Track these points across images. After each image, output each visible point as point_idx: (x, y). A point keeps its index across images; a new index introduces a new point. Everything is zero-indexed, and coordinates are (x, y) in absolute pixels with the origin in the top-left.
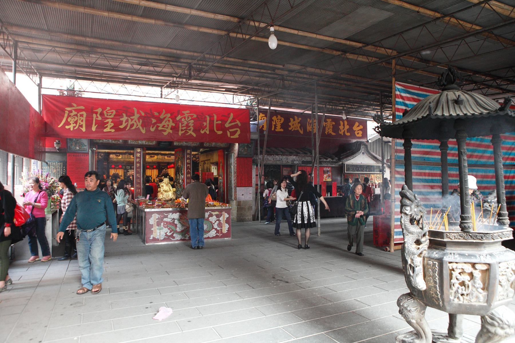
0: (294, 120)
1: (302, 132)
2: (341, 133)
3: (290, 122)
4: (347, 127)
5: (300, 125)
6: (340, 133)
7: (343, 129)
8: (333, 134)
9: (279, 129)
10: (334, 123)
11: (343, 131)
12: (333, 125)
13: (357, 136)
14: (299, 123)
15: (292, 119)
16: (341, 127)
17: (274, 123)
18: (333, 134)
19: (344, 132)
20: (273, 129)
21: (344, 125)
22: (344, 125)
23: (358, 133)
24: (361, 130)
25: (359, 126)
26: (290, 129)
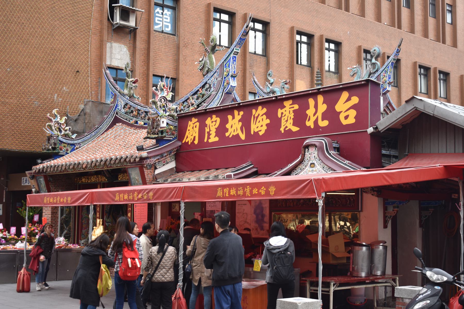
0: (233, 118)
1: (243, 137)
2: (310, 124)
3: (227, 122)
4: (322, 108)
5: (241, 123)
6: (308, 124)
7: (314, 115)
8: (295, 129)
9: (214, 139)
10: (296, 107)
11: (313, 119)
12: (294, 111)
13: (344, 122)
14: (239, 121)
15: (230, 117)
16: (310, 112)
17: (207, 130)
18: (295, 129)
19: (316, 122)
20: (206, 140)
21: (316, 106)
22: (316, 106)
23: (346, 117)
24: (353, 107)
25: (349, 99)
26: (227, 134)
